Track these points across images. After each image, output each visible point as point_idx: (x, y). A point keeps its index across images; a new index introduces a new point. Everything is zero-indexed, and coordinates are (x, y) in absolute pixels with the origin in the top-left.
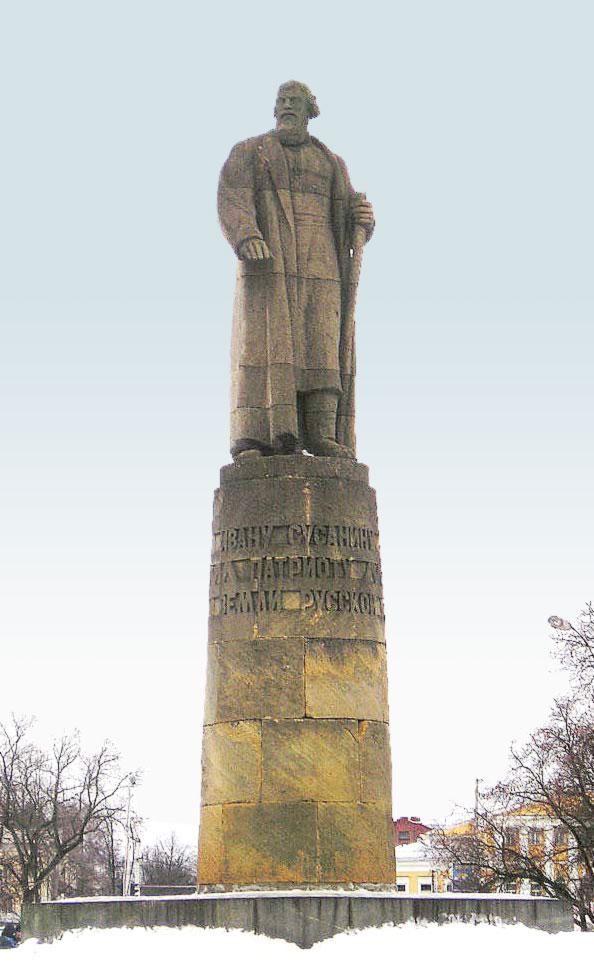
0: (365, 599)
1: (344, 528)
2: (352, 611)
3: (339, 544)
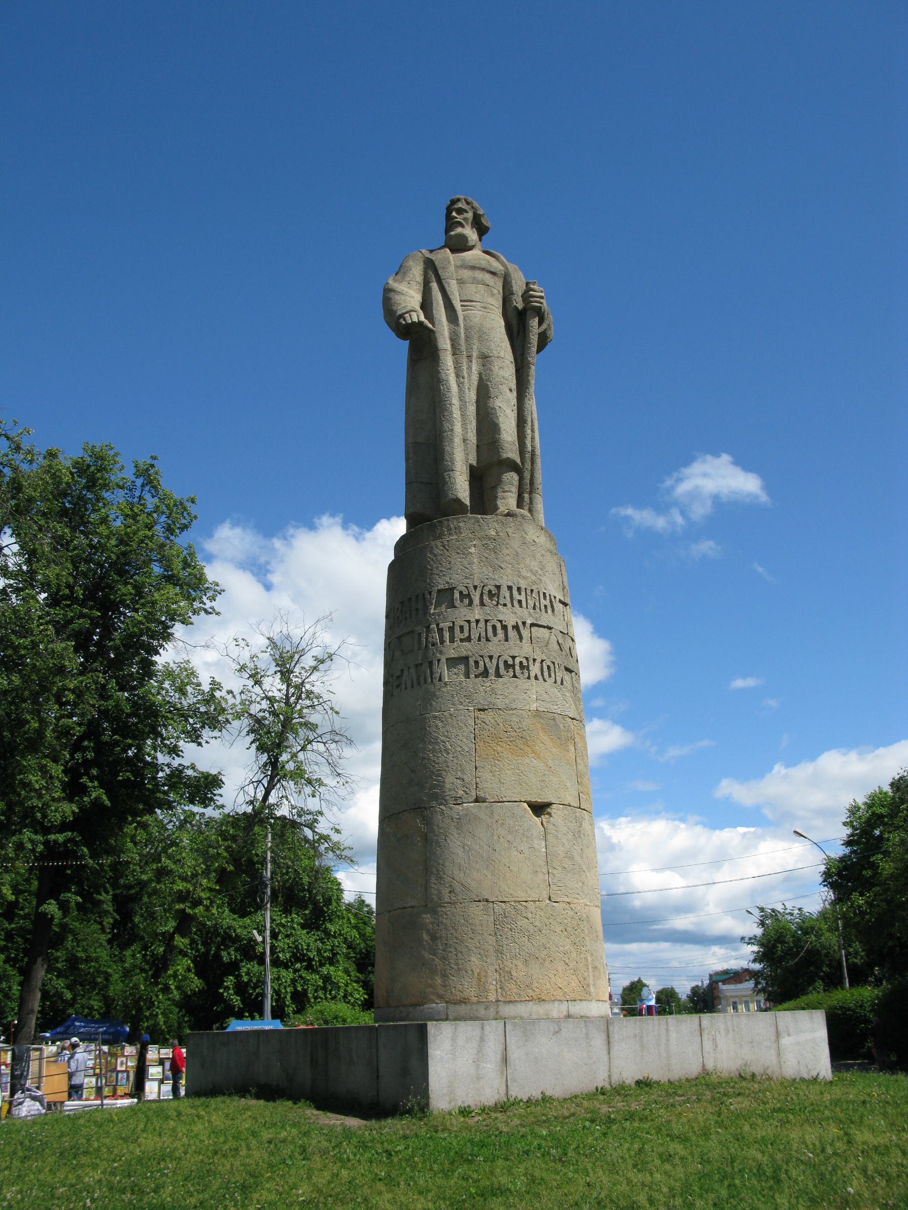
0: (549, 667)
1: (519, 589)
2: (533, 678)
3: (513, 606)
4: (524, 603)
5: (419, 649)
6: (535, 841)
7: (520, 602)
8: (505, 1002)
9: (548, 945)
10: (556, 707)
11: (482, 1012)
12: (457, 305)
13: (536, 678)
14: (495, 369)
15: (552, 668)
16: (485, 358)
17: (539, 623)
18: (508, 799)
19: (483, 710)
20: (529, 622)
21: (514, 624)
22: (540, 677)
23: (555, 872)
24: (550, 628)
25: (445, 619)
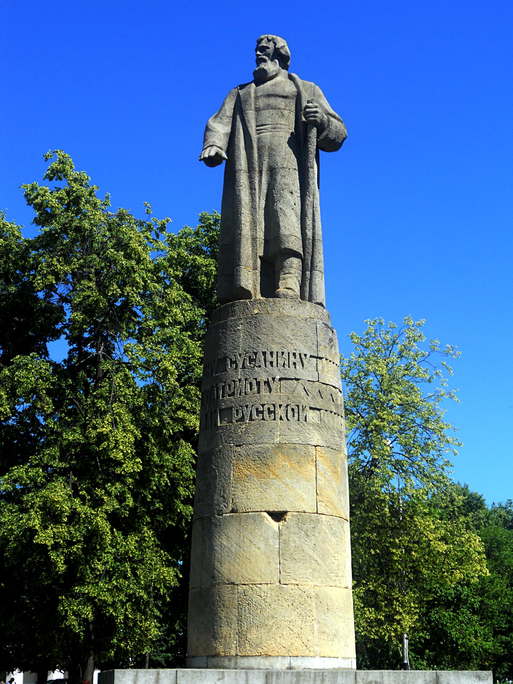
0: (293, 410)
1: (271, 353)
2: (278, 419)
4: (275, 364)
5: (207, 402)
6: (271, 540)
7: (271, 363)
8: (241, 656)
9: (276, 616)
10: (298, 439)
11: (227, 663)
12: (253, 130)
13: (281, 419)
14: (279, 178)
15: (296, 410)
16: (272, 171)
17: (287, 377)
18: (252, 510)
19: (240, 446)
20: (278, 377)
21: (265, 379)
22: (284, 418)
23: (285, 562)
24: (298, 380)
25: (221, 381)
